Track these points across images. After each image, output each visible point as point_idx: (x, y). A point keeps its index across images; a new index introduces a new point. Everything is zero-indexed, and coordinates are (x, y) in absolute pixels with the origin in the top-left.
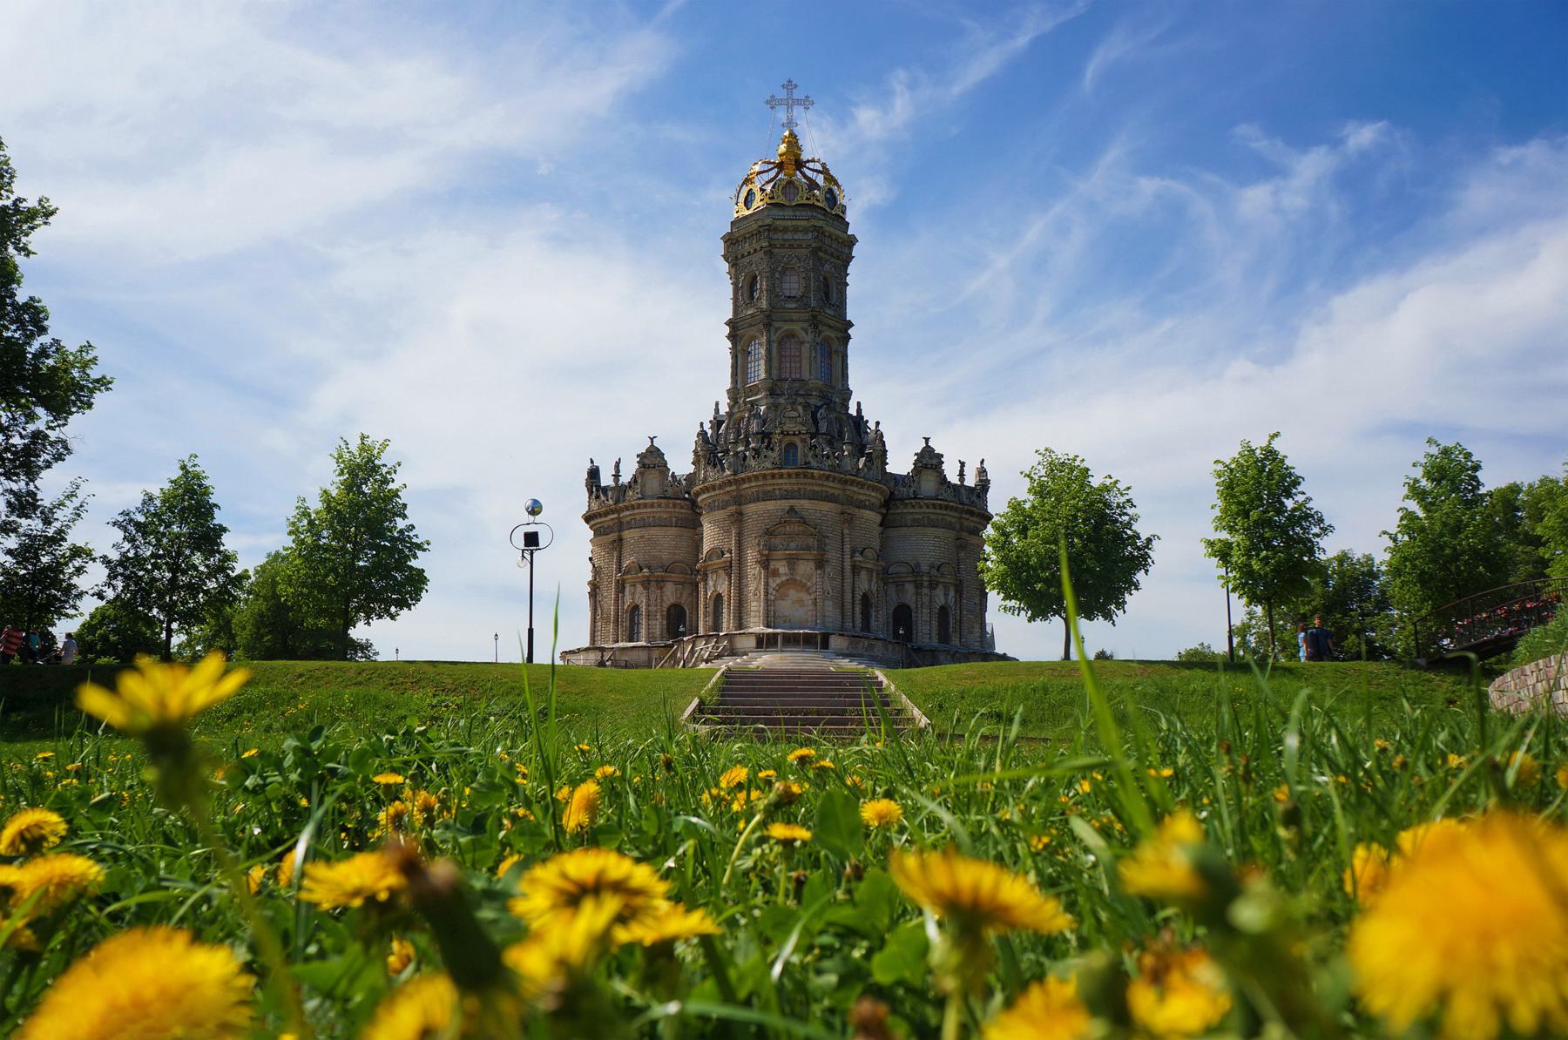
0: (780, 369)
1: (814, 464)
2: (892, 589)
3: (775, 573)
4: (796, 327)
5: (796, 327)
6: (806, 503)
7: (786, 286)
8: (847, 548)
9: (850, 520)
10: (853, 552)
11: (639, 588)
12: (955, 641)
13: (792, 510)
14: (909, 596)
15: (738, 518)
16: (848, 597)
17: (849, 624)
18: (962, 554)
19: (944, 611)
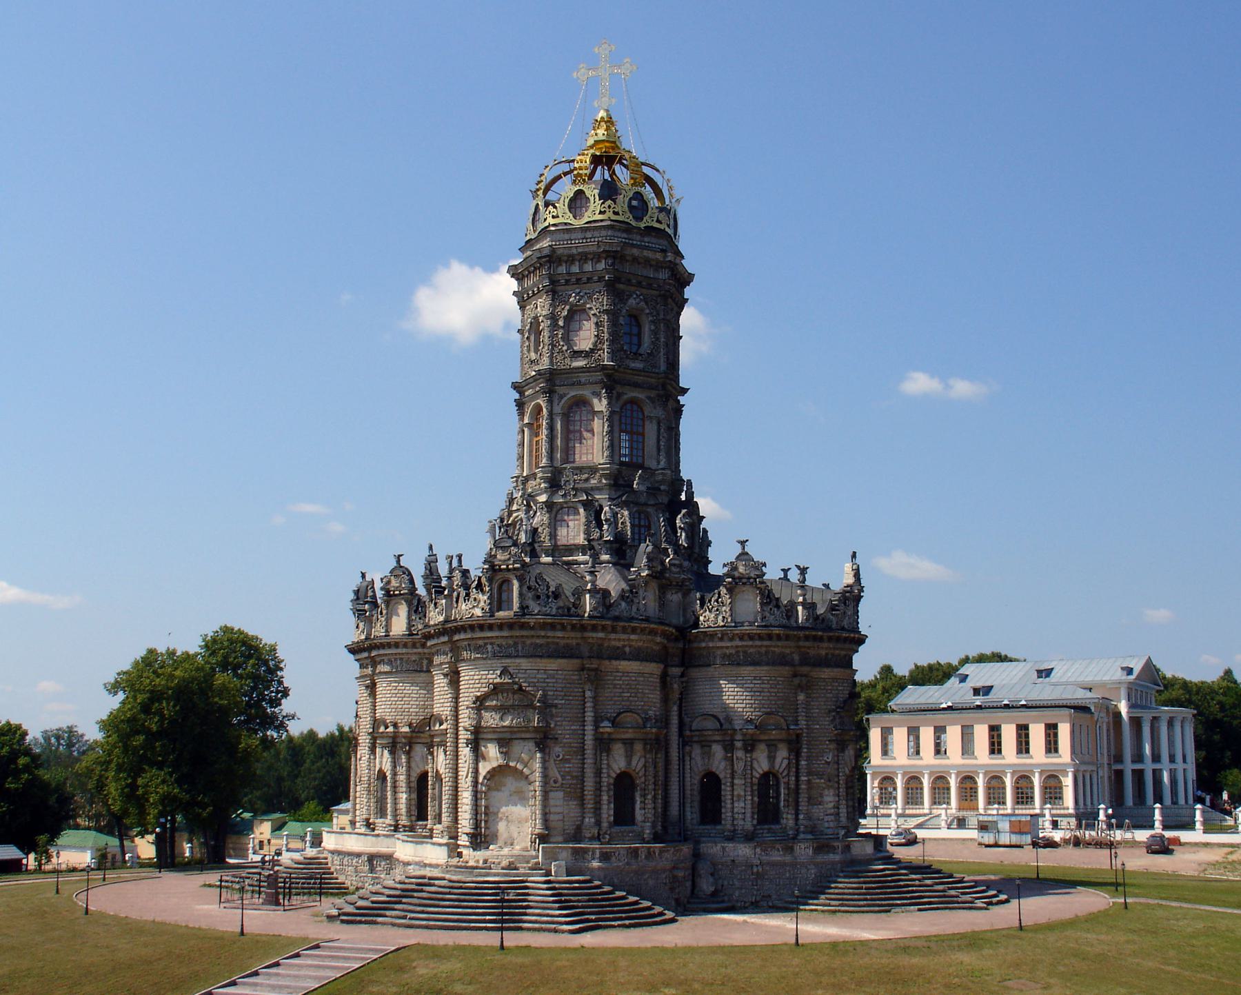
2: (697, 751)
5: (586, 392)
8: (589, 716)
9: (596, 678)
11: (386, 752)
14: (718, 764)
15: (454, 679)
16: (589, 784)
17: (589, 820)
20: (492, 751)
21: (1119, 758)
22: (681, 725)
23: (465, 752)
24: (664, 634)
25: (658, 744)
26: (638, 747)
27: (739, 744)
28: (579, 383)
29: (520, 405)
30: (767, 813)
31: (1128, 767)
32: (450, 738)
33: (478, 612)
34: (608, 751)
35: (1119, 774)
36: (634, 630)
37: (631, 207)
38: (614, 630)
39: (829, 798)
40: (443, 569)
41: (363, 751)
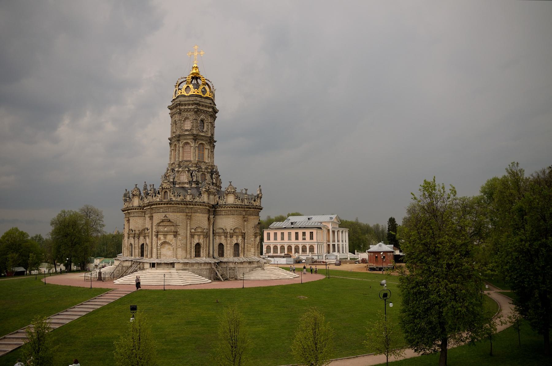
0: (183, 157)
1: (174, 199)
2: (217, 237)
3: (160, 239)
4: (188, 141)
6: (171, 214)
7: (186, 125)
8: (189, 228)
10: (191, 229)
12: (241, 255)
13: (166, 216)
14: (223, 241)
15: (151, 218)
17: (188, 256)
18: (246, 223)
19: (237, 245)
20: (161, 237)
21: (329, 241)
22: (213, 230)
23: (154, 238)
24: (209, 206)
25: (207, 236)
26: (202, 236)
27: (229, 236)
28: (187, 139)
29: (170, 144)
30: (236, 254)
31: (331, 243)
32: (150, 234)
33: (158, 200)
34: (193, 237)
35: (329, 245)
36: (201, 205)
37: (202, 91)
38: (195, 205)
39: (253, 250)
40: (149, 188)
41: (126, 238)
